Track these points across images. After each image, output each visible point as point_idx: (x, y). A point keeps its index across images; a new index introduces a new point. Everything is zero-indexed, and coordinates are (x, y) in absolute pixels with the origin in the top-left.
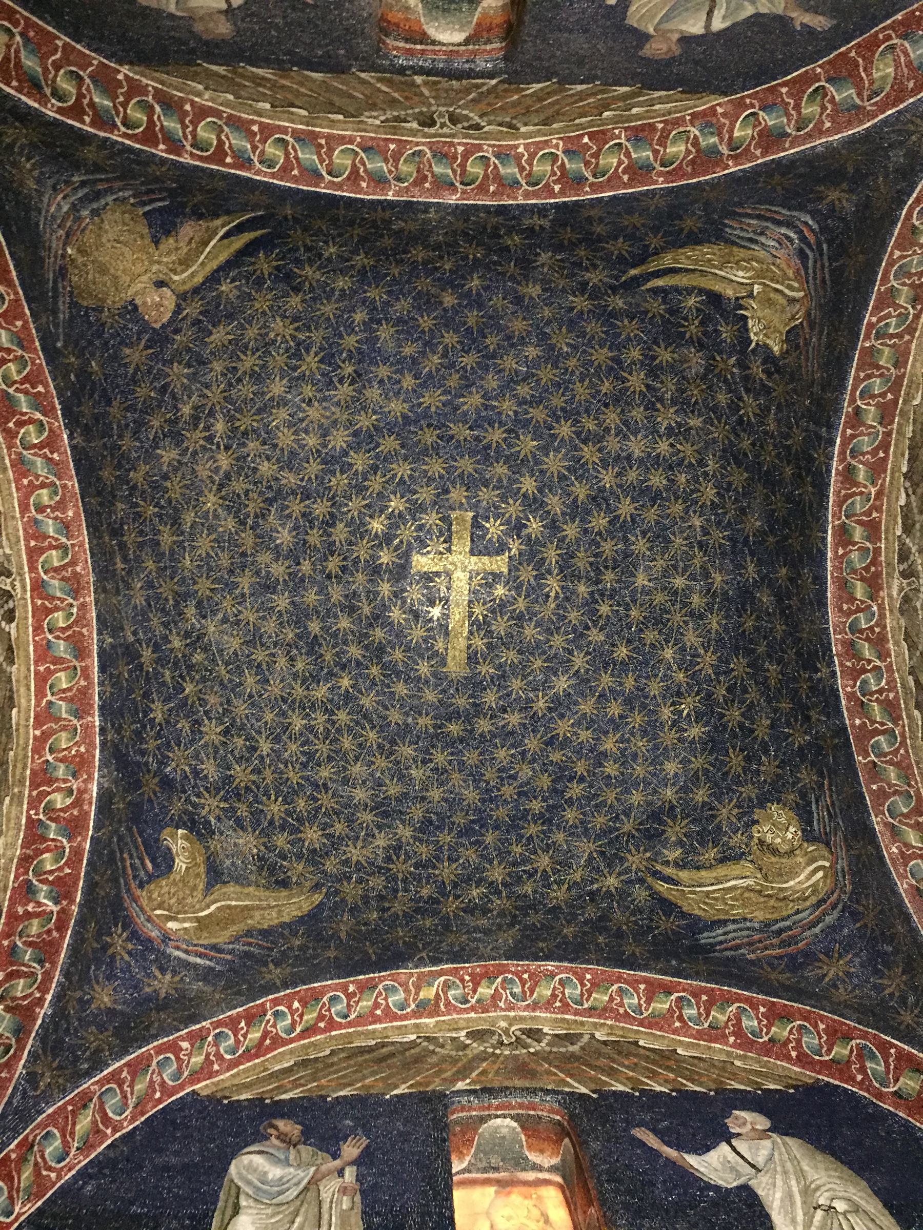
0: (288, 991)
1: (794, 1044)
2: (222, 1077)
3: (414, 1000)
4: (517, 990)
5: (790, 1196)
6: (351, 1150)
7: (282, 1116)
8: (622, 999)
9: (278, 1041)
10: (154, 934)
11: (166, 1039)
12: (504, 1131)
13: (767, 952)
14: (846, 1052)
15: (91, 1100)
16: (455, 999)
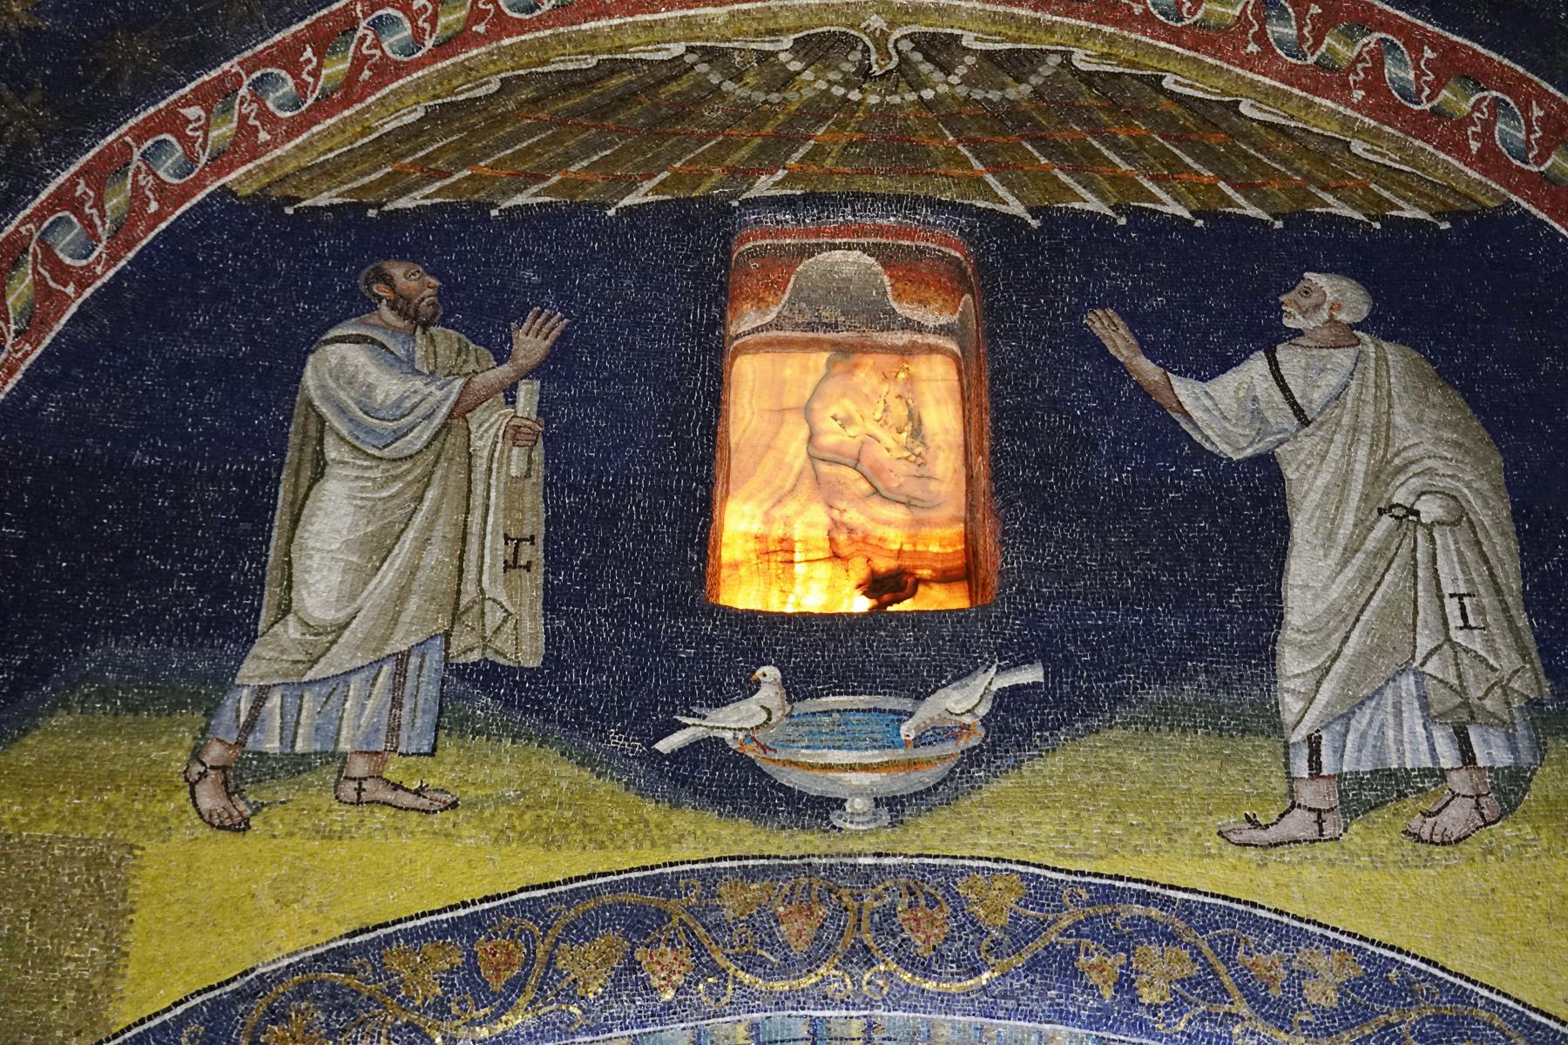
1: (1478, 129)
2: (278, 152)
5: (1344, 481)
6: (531, 344)
9: (386, 71)
11: (152, 110)
12: (848, 270)
15: (26, 251)
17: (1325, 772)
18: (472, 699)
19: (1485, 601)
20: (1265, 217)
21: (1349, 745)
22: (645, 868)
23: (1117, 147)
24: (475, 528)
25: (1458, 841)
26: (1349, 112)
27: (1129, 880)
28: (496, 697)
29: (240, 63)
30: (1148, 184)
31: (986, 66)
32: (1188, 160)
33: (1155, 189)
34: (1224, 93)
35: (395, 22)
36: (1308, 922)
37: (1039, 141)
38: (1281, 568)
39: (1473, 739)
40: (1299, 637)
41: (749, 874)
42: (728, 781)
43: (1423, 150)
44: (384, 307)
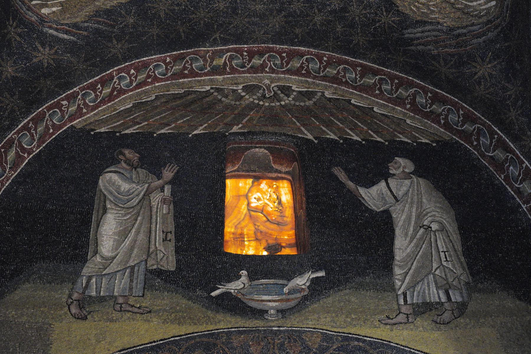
0: (127, 64)
1: (444, 117)
2: (89, 115)
3: (210, 66)
4: (278, 62)
6: (168, 174)
7: (128, 147)
8: (345, 74)
9: (121, 92)
10: (34, 18)
13: (447, 49)
14: (472, 129)
15: (14, 143)
16: (237, 65)
17: (408, 303)
18: (155, 280)
19: (452, 253)
20: (383, 141)
21: (415, 295)
22: (209, 331)
23: (339, 120)
24: (153, 229)
25: (447, 323)
26: (405, 111)
27: (353, 334)
28: (162, 279)
29: (79, 88)
30: (348, 131)
31: (300, 95)
32: (360, 124)
33: (350, 132)
34: (369, 105)
35: (124, 77)
36: (406, 347)
37: (316, 118)
38: (392, 244)
39: (451, 294)
40: (398, 263)
41: (240, 333)
42: (233, 305)
43: (427, 123)
44: (123, 163)
